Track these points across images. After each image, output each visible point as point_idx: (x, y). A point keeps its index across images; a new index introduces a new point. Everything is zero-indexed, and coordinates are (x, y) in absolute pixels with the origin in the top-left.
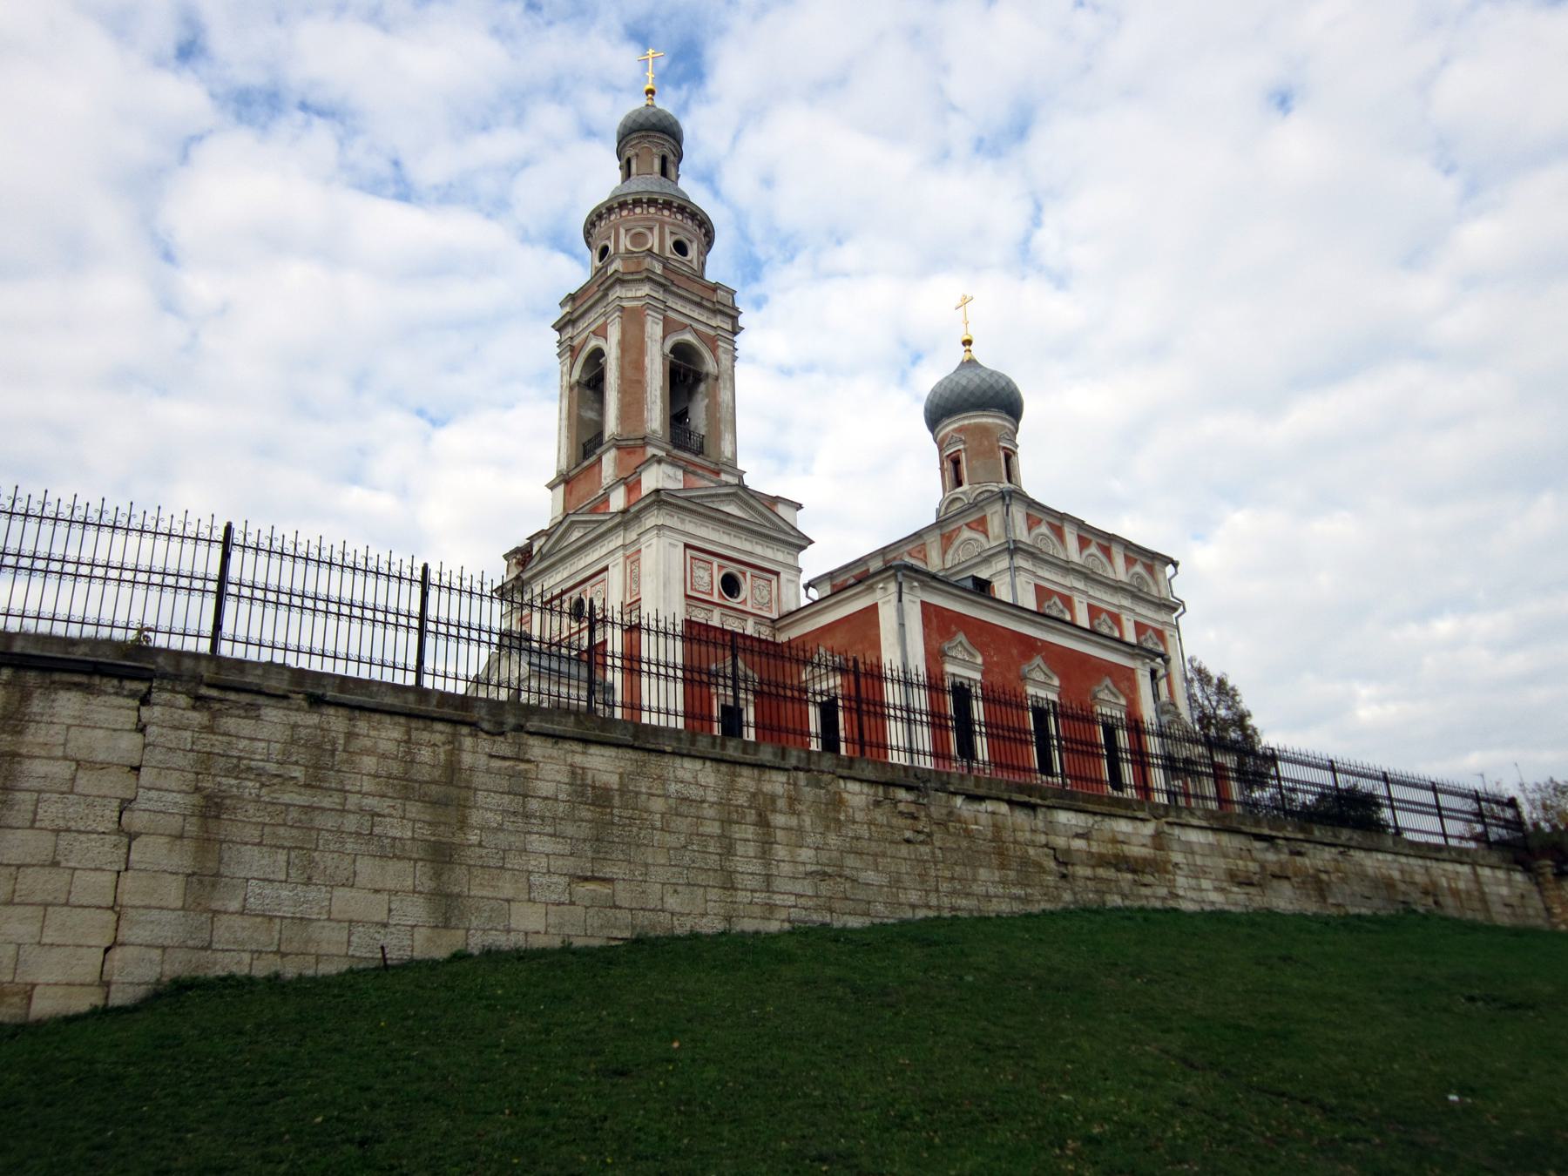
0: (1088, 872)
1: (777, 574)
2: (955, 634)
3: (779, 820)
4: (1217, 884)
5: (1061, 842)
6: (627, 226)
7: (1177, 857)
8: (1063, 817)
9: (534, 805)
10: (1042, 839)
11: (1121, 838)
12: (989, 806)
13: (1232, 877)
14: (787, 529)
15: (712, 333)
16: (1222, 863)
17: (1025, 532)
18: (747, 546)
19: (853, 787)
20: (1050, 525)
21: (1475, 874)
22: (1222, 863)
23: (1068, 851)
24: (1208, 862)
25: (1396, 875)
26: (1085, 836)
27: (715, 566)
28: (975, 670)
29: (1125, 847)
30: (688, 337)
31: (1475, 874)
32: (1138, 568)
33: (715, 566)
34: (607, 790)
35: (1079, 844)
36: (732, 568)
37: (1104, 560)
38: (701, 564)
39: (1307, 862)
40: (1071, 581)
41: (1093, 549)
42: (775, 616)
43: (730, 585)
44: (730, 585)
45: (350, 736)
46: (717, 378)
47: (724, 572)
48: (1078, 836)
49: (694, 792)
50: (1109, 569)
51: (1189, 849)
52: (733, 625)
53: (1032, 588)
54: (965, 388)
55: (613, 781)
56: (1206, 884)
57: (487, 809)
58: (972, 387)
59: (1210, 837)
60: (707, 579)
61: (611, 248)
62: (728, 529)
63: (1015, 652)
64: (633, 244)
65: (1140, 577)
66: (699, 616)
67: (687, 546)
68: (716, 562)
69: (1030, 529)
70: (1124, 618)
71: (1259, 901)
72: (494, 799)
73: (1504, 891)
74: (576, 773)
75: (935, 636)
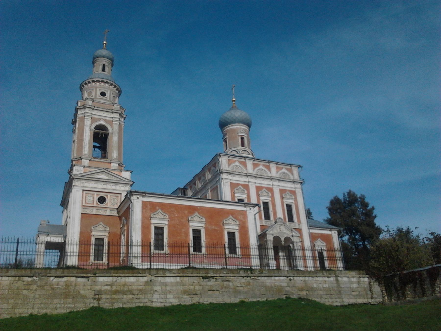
0: (108, 297)
1: (121, 194)
2: (158, 209)
4: (176, 295)
5: (97, 288)
7: (158, 288)
8: (101, 279)
11: (128, 284)
12: (65, 279)
13: (185, 292)
14: (124, 179)
15: (112, 119)
16: (181, 288)
17: (227, 166)
18: (109, 187)
20: (240, 162)
21: (337, 280)
22: (181, 288)
25: (284, 285)
26: (111, 285)
27: (95, 195)
28: (166, 221)
29: (130, 287)
31: (337, 280)
32: (284, 170)
33: (95, 195)
35: (108, 288)
37: (266, 170)
38: (90, 195)
39: (231, 284)
40: (246, 179)
41: (261, 167)
43: (102, 200)
44: (102, 200)
46: (112, 133)
47: (99, 196)
48: (107, 285)
50: (269, 172)
51: (166, 284)
53: (229, 184)
56: (168, 296)
60: (92, 199)
62: (100, 183)
63: (186, 212)
65: (284, 173)
66: (88, 211)
67: (83, 190)
68: (96, 193)
69: (229, 165)
70: (274, 189)
71: (195, 300)
73: (355, 286)
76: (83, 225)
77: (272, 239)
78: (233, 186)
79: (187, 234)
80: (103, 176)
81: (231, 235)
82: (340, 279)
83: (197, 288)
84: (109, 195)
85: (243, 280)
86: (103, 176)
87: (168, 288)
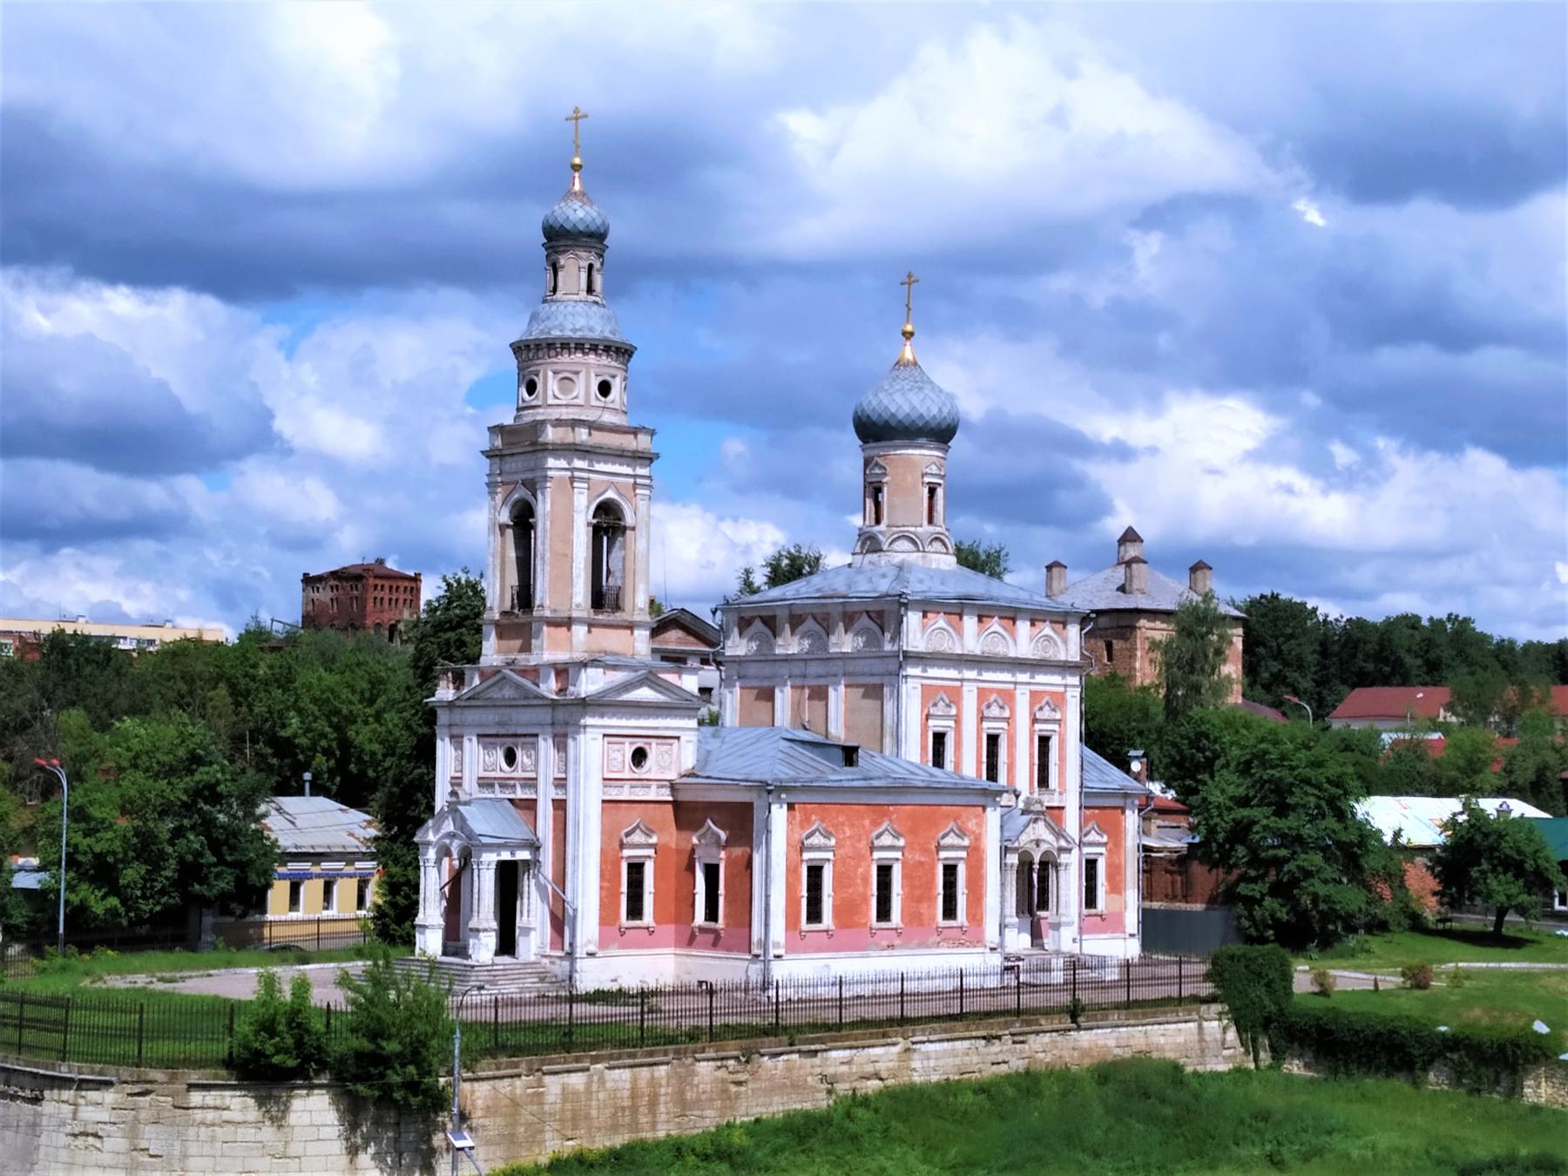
1: (678, 738)
3: (663, 1091)
5: (830, 1071)
6: (559, 367)
8: (834, 1054)
9: (547, 1108)
10: (819, 1070)
17: (919, 635)
19: (703, 1064)
21: (1200, 1027)
23: (834, 1076)
24: (941, 1063)
25: (1112, 1043)
26: (849, 1063)
30: (610, 494)
31: (1200, 1027)
34: (576, 1093)
35: (845, 1068)
36: (640, 743)
42: (672, 775)
43: (639, 756)
44: (639, 756)
45: (473, 1092)
49: (621, 1085)
52: (640, 795)
54: (893, 415)
55: (581, 1088)
57: (526, 1114)
58: (900, 416)
59: (946, 1045)
60: (620, 759)
61: (540, 387)
63: (867, 822)
64: (561, 389)
66: (614, 794)
72: (530, 1108)
74: (564, 1088)
75: (797, 828)
76: (607, 833)
77: (1016, 861)
78: (928, 693)
79: (866, 880)
80: (645, 694)
81: (950, 870)
82: (1205, 1024)
83: (975, 1059)
84: (654, 741)
85: (1046, 1038)
86: (645, 694)
87: (932, 1063)
